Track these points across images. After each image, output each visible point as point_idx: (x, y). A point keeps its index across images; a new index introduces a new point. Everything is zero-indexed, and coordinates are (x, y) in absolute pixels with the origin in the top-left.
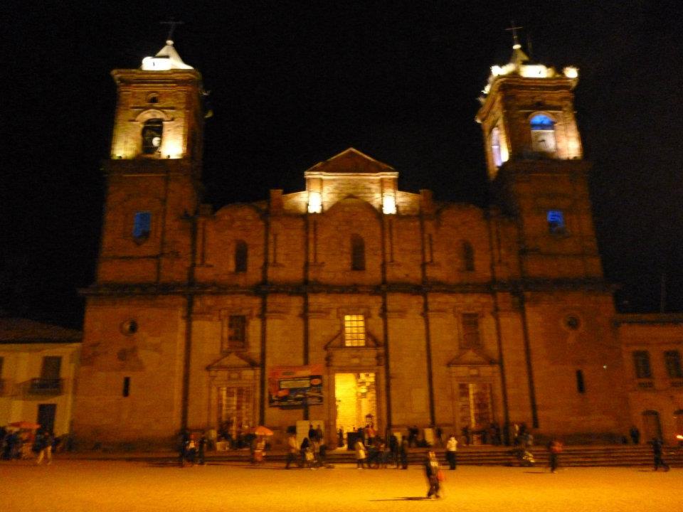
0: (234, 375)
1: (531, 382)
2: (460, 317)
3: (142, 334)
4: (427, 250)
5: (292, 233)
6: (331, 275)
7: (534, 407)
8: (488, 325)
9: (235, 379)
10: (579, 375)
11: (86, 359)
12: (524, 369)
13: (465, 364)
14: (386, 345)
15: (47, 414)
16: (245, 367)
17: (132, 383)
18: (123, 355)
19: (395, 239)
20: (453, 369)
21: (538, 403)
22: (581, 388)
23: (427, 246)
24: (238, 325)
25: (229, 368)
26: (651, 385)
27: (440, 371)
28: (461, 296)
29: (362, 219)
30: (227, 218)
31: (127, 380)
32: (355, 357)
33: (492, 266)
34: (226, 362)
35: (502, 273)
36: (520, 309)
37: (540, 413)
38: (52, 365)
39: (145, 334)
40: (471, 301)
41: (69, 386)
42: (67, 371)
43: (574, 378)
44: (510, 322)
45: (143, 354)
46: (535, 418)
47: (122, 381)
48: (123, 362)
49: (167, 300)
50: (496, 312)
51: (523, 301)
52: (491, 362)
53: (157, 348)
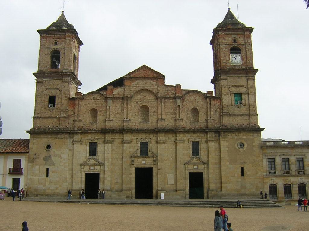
2: (191, 143)
3: (53, 150)
4: (177, 113)
5: (117, 105)
7: (221, 183)
8: (202, 147)
9: (92, 169)
10: (242, 168)
11: (32, 161)
12: (218, 166)
13: (192, 164)
14: (157, 156)
15: (16, 182)
18: (45, 159)
19: (163, 108)
20: (186, 166)
21: (223, 181)
22: (243, 174)
23: (177, 111)
25: (90, 166)
26: (275, 173)
27: (180, 167)
28: (192, 134)
30: (89, 98)
31: (48, 169)
32: (144, 160)
33: (207, 120)
35: (212, 124)
37: (223, 185)
38: (17, 163)
39: (54, 150)
40: (195, 137)
42: (23, 165)
43: (240, 170)
44: (213, 146)
45: (53, 158)
46: (221, 187)
47: (46, 169)
49: (63, 136)
50: (207, 142)
51: (219, 136)
52: (204, 163)
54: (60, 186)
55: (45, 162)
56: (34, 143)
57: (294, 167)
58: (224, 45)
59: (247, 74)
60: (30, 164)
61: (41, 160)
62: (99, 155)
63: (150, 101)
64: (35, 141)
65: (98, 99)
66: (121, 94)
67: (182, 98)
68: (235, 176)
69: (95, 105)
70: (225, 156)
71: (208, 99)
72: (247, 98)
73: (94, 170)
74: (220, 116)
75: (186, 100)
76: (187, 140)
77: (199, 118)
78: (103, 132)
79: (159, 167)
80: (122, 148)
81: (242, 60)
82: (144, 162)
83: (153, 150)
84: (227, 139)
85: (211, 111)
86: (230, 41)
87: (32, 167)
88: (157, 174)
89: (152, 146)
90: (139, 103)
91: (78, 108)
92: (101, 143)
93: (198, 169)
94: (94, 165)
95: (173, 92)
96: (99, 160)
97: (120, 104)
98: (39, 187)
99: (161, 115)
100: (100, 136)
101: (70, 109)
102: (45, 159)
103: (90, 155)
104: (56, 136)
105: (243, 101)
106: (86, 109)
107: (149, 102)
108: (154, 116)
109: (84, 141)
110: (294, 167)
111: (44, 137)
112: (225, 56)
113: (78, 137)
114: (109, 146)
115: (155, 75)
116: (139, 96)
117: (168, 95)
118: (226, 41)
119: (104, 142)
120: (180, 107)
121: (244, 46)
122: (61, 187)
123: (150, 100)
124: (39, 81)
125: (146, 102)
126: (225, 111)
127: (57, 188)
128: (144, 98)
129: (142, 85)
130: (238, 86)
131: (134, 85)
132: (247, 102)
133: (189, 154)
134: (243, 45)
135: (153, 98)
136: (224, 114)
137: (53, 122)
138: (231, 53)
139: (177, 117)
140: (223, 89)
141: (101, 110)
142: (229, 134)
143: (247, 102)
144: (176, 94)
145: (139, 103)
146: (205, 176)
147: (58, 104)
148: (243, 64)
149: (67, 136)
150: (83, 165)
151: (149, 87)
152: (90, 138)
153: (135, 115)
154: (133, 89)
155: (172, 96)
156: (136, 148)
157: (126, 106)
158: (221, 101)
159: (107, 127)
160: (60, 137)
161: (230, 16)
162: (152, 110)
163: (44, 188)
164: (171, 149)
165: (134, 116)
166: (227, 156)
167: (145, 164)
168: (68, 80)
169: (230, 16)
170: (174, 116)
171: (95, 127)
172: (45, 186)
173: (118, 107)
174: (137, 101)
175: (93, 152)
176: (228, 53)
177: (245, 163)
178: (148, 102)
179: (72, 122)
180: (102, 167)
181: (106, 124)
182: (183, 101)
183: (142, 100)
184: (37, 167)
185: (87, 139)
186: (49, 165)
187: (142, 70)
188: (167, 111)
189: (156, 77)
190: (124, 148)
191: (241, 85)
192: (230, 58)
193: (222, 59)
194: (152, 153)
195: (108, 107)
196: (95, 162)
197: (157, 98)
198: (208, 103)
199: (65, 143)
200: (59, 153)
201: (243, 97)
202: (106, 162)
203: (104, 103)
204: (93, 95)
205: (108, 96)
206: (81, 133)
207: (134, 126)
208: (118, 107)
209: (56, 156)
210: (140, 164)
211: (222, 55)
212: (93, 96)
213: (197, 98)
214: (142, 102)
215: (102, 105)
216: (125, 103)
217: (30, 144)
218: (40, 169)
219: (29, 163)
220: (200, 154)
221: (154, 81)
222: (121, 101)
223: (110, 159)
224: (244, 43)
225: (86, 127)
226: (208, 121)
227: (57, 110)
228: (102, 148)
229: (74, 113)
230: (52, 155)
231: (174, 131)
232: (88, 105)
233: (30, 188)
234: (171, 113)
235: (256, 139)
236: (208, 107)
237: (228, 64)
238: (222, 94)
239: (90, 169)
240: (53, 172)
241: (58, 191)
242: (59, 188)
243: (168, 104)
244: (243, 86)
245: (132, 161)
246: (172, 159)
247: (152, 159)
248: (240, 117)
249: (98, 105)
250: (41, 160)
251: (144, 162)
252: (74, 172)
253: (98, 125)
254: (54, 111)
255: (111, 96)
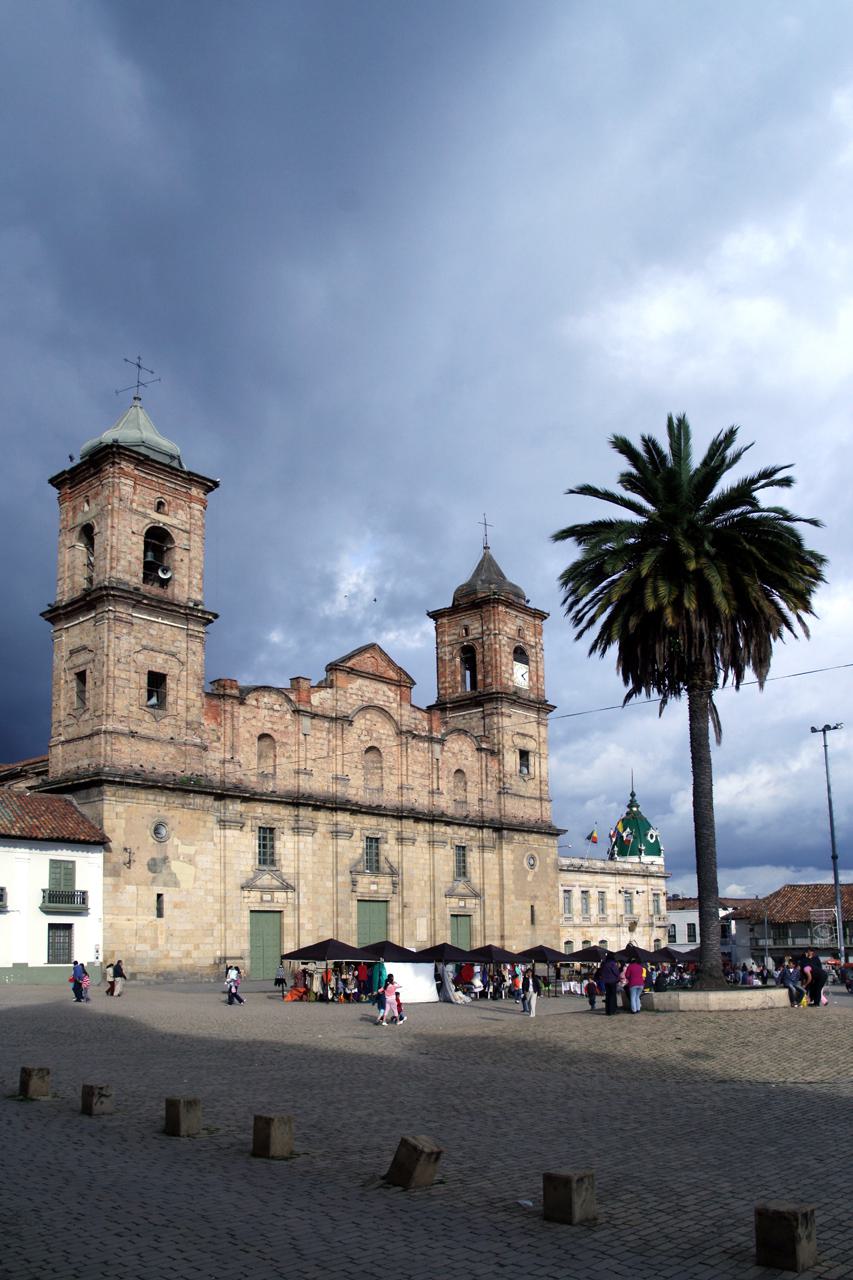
0: (267, 897)
1: (502, 915)
5: (319, 735)
6: (353, 791)
8: (473, 857)
9: (268, 901)
11: (111, 871)
16: (278, 889)
17: (166, 898)
18: (154, 866)
19: (409, 759)
21: (506, 933)
22: (533, 921)
23: (435, 771)
24: (267, 835)
25: (264, 890)
27: (441, 900)
29: (382, 731)
30: (254, 703)
31: (159, 896)
32: (374, 883)
34: (258, 883)
35: (490, 811)
36: (497, 847)
39: (175, 839)
41: (95, 902)
43: (530, 911)
48: (153, 875)
49: (199, 800)
50: (482, 848)
51: (501, 838)
52: (476, 895)
53: (191, 861)
54: (197, 947)
55: (151, 875)
56: (117, 814)
57: (594, 909)
58: (506, 639)
59: (539, 710)
60: (110, 880)
61: (140, 869)
62: (283, 862)
63: (384, 737)
64: (120, 808)
65: (276, 707)
66: (326, 706)
67: (442, 742)
68: (522, 924)
69: (270, 725)
70: (509, 882)
71: (483, 755)
72: (537, 764)
73: (273, 904)
74: (499, 793)
75: (446, 748)
76: (449, 841)
77: (468, 795)
78: (297, 801)
79: (405, 900)
80: (331, 848)
81: (530, 679)
82: (374, 887)
83: (390, 859)
84: (511, 847)
85: (487, 781)
86: (512, 632)
87: (116, 887)
88: (402, 916)
89: (390, 850)
90: (363, 738)
91: (233, 725)
92: (286, 831)
93: (465, 907)
94: (271, 890)
95: (425, 724)
96: (285, 877)
97: (325, 733)
98: (139, 951)
99: (407, 775)
100: (285, 812)
101: (209, 724)
102: (154, 866)
103: (260, 863)
104: (178, 801)
105: (531, 769)
106: (249, 732)
107: (381, 739)
108: (392, 777)
109: (249, 823)
110: (594, 909)
111: (148, 800)
112: (507, 663)
113: (236, 808)
114: (307, 841)
115: (392, 674)
116: (363, 721)
117: (416, 730)
118: (508, 630)
119: (297, 830)
120: (440, 764)
121: (533, 650)
122: (199, 948)
123: (384, 732)
124: (120, 615)
125: (376, 740)
126: (507, 786)
127: (188, 954)
128: (373, 728)
129: (368, 695)
130: (524, 735)
131: (354, 691)
132: (537, 773)
133: (452, 874)
134: (532, 647)
135: (390, 733)
136: (509, 791)
137: (166, 754)
138: (515, 660)
139: (435, 787)
140: (506, 737)
141: (284, 740)
142: (516, 837)
143: (537, 773)
144: (431, 730)
145: (363, 738)
146: (477, 921)
147: (176, 702)
148: (531, 688)
149: (209, 801)
150: (247, 886)
151: (382, 703)
152: (261, 811)
153: (356, 767)
154: (350, 701)
155: (423, 734)
156: (360, 851)
157: (339, 742)
158: (501, 763)
159: (301, 791)
160: (190, 804)
161: (487, 566)
162: (389, 760)
163: (152, 954)
164: (422, 861)
165: (354, 770)
166: (511, 882)
167: (376, 892)
168: (201, 635)
169: (487, 566)
170: (427, 782)
171: (269, 787)
172: (155, 946)
173: (321, 741)
174: (359, 732)
175: (266, 855)
176: (511, 657)
177: (535, 897)
178: (379, 739)
179: (216, 764)
180: (290, 895)
181: (301, 782)
182: (442, 750)
183: (369, 732)
184: (131, 889)
185: (256, 818)
186: (165, 885)
187: (369, 655)
188: (415, 768)
189: (400, 681)
190: (339, 850)
191: (530, 734)
192: (512, 669)
193: (503, 668)
194: (391, 867)
195: (302, 737)
196: (276, 883)
197: (400, 733)
198: (484, 764)
199: (205, 822)
200: (191, 850)
201: (531, 759)
202: (302, 882)
203: (290, 723)
204: (264, 697)
205: (302, 708)
206: (245, 800)
207: (355, 795)
208: (321, 741)
209: (181, 859)
210: (366, 891)
211: (504, 660)
212: (266, 700)
213: (464, 747)
214: (368, 738)
215: (286, 727)
216: (339, 735)
217: (106, 814)
218: (137, 893)
219: (105, 876)
220: (468, 875)
221: (390, 690)
222: (327, 725)
223: (310, 877)
224: (533, 644)
225: (250, 781)
226: (485, 803)
227: (173, 722)
228: (290, 845)
229: (219, 738)
230: (170, 856)
231: (433, 818)
232: (254, 722)
233: (113, 952)
234: (422, 776)
235: (550, 850)
236: (484, 772)
237: (510, 683)
238: (503, 746)
239: (262, 898)
240: (176, 906)
241: (190, 961)
242: (195, 954)
243: (416, 753)
244: (531, 737)
245: (354, 883)
246: (423, 884)
247: (388, 880)
248: (528, 802)
249: (275, 727)
250: (140, 869)
251: (374, 887)
252: (228, 908)
253: (278, 782)
254: (166, 721)
255: (309, 710)
